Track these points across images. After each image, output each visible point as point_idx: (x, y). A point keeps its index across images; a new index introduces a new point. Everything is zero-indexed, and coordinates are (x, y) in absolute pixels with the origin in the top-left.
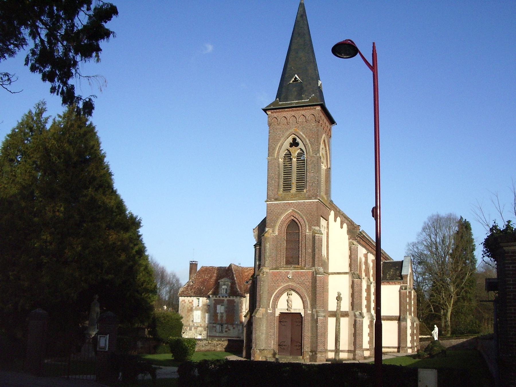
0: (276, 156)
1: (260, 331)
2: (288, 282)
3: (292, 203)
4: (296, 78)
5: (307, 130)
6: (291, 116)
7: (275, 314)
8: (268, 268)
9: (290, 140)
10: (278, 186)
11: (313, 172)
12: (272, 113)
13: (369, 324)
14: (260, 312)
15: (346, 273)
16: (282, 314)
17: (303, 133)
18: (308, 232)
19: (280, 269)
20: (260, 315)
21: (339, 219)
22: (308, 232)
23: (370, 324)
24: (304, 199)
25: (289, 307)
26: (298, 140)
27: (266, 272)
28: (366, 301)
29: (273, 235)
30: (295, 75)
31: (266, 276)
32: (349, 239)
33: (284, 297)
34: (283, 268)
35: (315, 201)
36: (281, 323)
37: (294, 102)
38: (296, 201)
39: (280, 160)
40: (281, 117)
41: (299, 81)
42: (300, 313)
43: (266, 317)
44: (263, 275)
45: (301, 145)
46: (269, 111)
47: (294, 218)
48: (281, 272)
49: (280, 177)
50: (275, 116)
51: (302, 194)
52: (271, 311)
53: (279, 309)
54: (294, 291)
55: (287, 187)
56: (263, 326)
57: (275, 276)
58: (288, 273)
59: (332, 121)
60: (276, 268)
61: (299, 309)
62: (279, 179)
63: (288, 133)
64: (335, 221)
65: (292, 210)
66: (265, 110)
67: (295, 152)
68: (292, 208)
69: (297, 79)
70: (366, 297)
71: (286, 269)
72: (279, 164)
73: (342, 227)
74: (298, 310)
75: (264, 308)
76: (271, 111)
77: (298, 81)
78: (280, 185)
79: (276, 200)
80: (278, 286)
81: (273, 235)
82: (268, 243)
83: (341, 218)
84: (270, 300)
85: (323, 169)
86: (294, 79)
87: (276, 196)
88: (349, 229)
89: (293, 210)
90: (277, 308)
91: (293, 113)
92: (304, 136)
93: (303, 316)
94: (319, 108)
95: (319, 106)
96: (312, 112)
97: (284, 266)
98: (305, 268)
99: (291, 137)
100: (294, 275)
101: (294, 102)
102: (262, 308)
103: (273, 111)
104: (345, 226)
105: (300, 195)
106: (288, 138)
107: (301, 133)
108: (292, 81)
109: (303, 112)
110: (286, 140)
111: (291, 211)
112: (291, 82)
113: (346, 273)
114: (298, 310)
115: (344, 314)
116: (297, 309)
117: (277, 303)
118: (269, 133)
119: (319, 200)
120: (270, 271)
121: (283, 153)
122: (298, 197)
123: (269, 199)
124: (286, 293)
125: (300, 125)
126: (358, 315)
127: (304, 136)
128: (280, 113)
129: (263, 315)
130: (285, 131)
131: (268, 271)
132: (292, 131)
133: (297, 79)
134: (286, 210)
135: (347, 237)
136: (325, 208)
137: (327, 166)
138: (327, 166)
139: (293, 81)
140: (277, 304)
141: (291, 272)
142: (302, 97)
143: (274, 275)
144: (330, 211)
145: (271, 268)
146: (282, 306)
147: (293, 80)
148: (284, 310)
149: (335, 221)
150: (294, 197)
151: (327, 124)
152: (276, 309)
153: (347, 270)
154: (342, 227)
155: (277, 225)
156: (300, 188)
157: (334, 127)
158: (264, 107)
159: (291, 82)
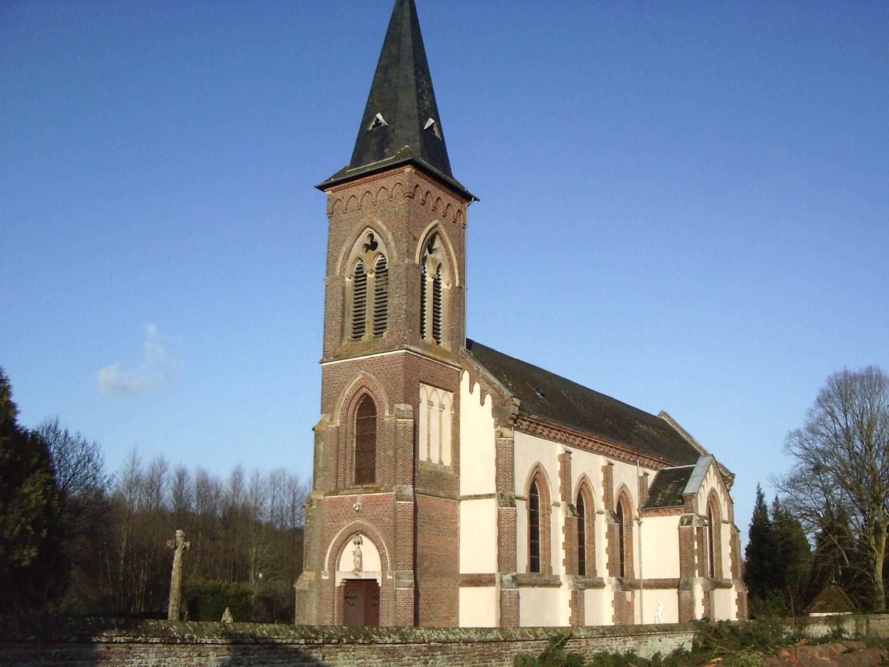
0: (338, 274)
1: (304, 617)
2: (354, 518)
3: (362, 360)
4: (378, 120)
5: (391, 214)
6: (364, 192)
7: (334, 582)
8: (322, 491)
9: (364, 239)
10: (342, 330)
11: (397, 295)
12: (333, 191)
13: (570, 599)
14: (305, 579)
15: (490, 496)
16: (349, 582)
17: (384, 223)
18: (387, 417)
19: (341, 492)
20: (304, 586)
21: (477, 387)
22: (387, 417)
23: (572, 598)
24: (380, 351)
25: (359, 569)
26: (377, 237)
27: (317, 500)
28: (564, 551)
29: (332, 426)
30: (374, 115)
31: (317, 509)
32: (496, 426)
33: (350, 547)
34: (346, 492)
35: (400, 353)
36: (349, 600)
37: (371, 164)
38: (369, 357)
39: (347, 279)
40: (348, 197)
41: (383, 125)
42: (375, 580)
43: (318, 588)
44: (311, 505)
45: (381, 248)
46: (329, 189)
47: (367, 390)
48: (343, 499)
49: (346, 314)
50: (339, 197)
51: (379, 342)
52: (327, 578)
53: (342, 572)
54: (365, 535)
55: (359, 329)
56: (311, 606)
57: (334, 507)
58: (354, 500)
59: (466, 197)
60: (335, 493)
61: (374, 572)
62: (343, 316)
63: (358, 226)
64: (471, 391)
65: (364, 375)
66: (322, 188)
67: (371, 264)
68: (363, 371)
69: (380, 122)
70: (563, 543)
71: (351, 491)
72: (344, 288)
73: (482, 403)
74: (372, 574)
75: (312, 570)
76: (331, 188)
77: (381, 124)
78: (346, 327)
79: (337, 357)
80: (340, 527)
81: (332, 426)
82: (322, 444)
83: (480, 385)
84: (325, 555)
85: (444, 289)
86: (375, 122)
87: (338, 350)
88: (495, 406)
89: (364, 375)
90: (338, 569)
91: (367, 187)
92: (384, 228)
93: (380, 585)
94: (408, 169)
95: (408, 164)
96: (399, 178)
97: (351, 487)
98: (383, 489)
99: (364, 233)
100: (365, 502)
101: (371, 164)
102: (309, 570)
103: (334, 188)
104: (488, 399)
105: (376, 345)
106: (359, 236)
107: (380, 223)
108: (371, 126)
109: (383, 182)
110: (356, 240)
111: (360, 376)
112: (371, 128)
113: (490, 496)
114: (372, 574)
115: (486, 579)
116: (370, 572)
117: (339, 560)
118: (330, 230)
119: (407, 349)
120: (326, 497)
121: (351, 269)
122: (372, 349)
123: (326, 357)
124: (351, 543)
125: (379, 208)
126: (508, 581)
127: (384, 228)
128: (346, 190)
129: (310, 585)
130: (355, 223)
131: (322, 497)
132: (365, 221)
133: (380, 122)
134: (354, 376)
135: (491, 421)
136: (440, 367)
137: (454, 284)
138: (454, 284)
139: (374, 126)
140: (339, 563)
141: (358, 498)
142: (384, 153)
143: (333, 504)
144: (461, 373)
145: (327, 491)
146: (346, 569)
147: (374, 123)
148: (349, 574)
149: (471, 391)
150: (368, 348)
151: (457, 204)
152: (337, 573)
153: (493, 490)
154: (482, 403)
155: (337, 406)
156: (379, 329)
157: (472, 209)
158: (321, 181)
159: (371, 128)
